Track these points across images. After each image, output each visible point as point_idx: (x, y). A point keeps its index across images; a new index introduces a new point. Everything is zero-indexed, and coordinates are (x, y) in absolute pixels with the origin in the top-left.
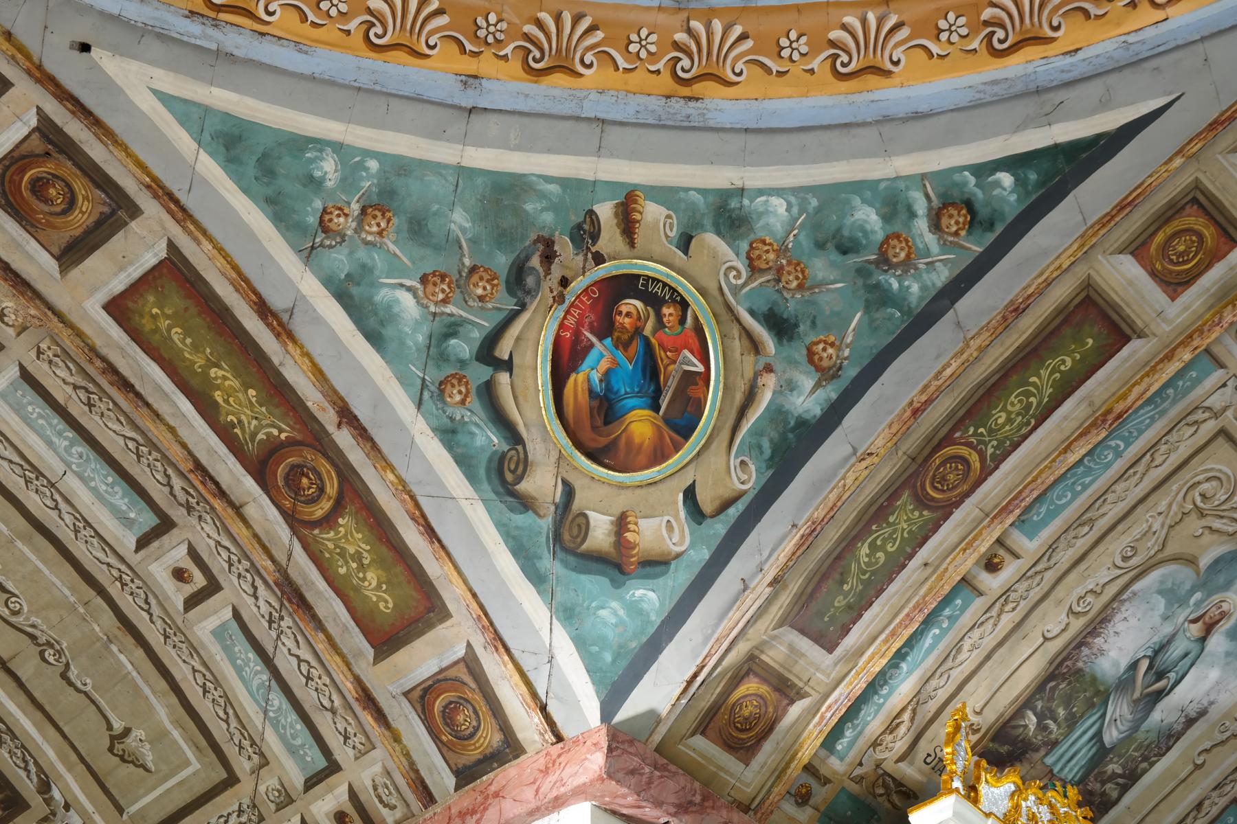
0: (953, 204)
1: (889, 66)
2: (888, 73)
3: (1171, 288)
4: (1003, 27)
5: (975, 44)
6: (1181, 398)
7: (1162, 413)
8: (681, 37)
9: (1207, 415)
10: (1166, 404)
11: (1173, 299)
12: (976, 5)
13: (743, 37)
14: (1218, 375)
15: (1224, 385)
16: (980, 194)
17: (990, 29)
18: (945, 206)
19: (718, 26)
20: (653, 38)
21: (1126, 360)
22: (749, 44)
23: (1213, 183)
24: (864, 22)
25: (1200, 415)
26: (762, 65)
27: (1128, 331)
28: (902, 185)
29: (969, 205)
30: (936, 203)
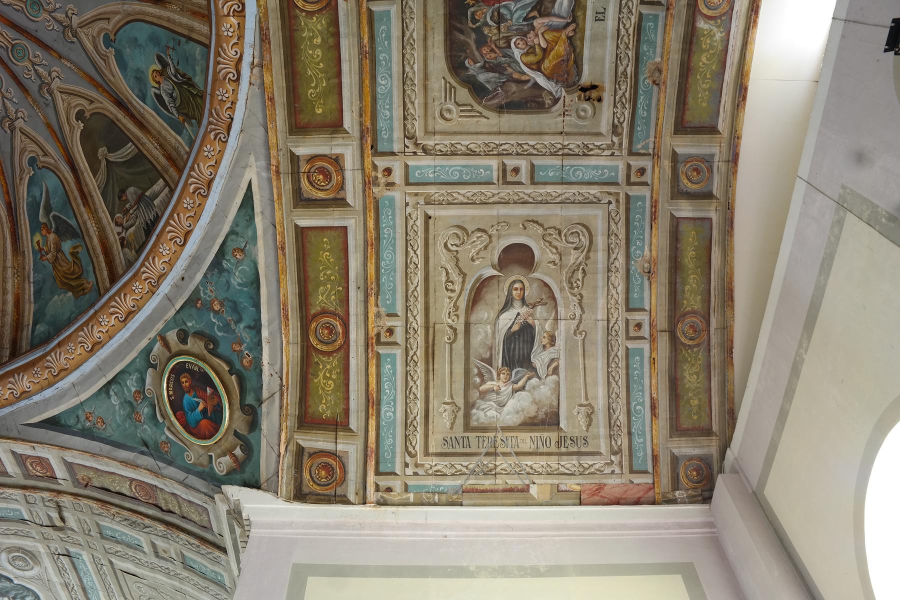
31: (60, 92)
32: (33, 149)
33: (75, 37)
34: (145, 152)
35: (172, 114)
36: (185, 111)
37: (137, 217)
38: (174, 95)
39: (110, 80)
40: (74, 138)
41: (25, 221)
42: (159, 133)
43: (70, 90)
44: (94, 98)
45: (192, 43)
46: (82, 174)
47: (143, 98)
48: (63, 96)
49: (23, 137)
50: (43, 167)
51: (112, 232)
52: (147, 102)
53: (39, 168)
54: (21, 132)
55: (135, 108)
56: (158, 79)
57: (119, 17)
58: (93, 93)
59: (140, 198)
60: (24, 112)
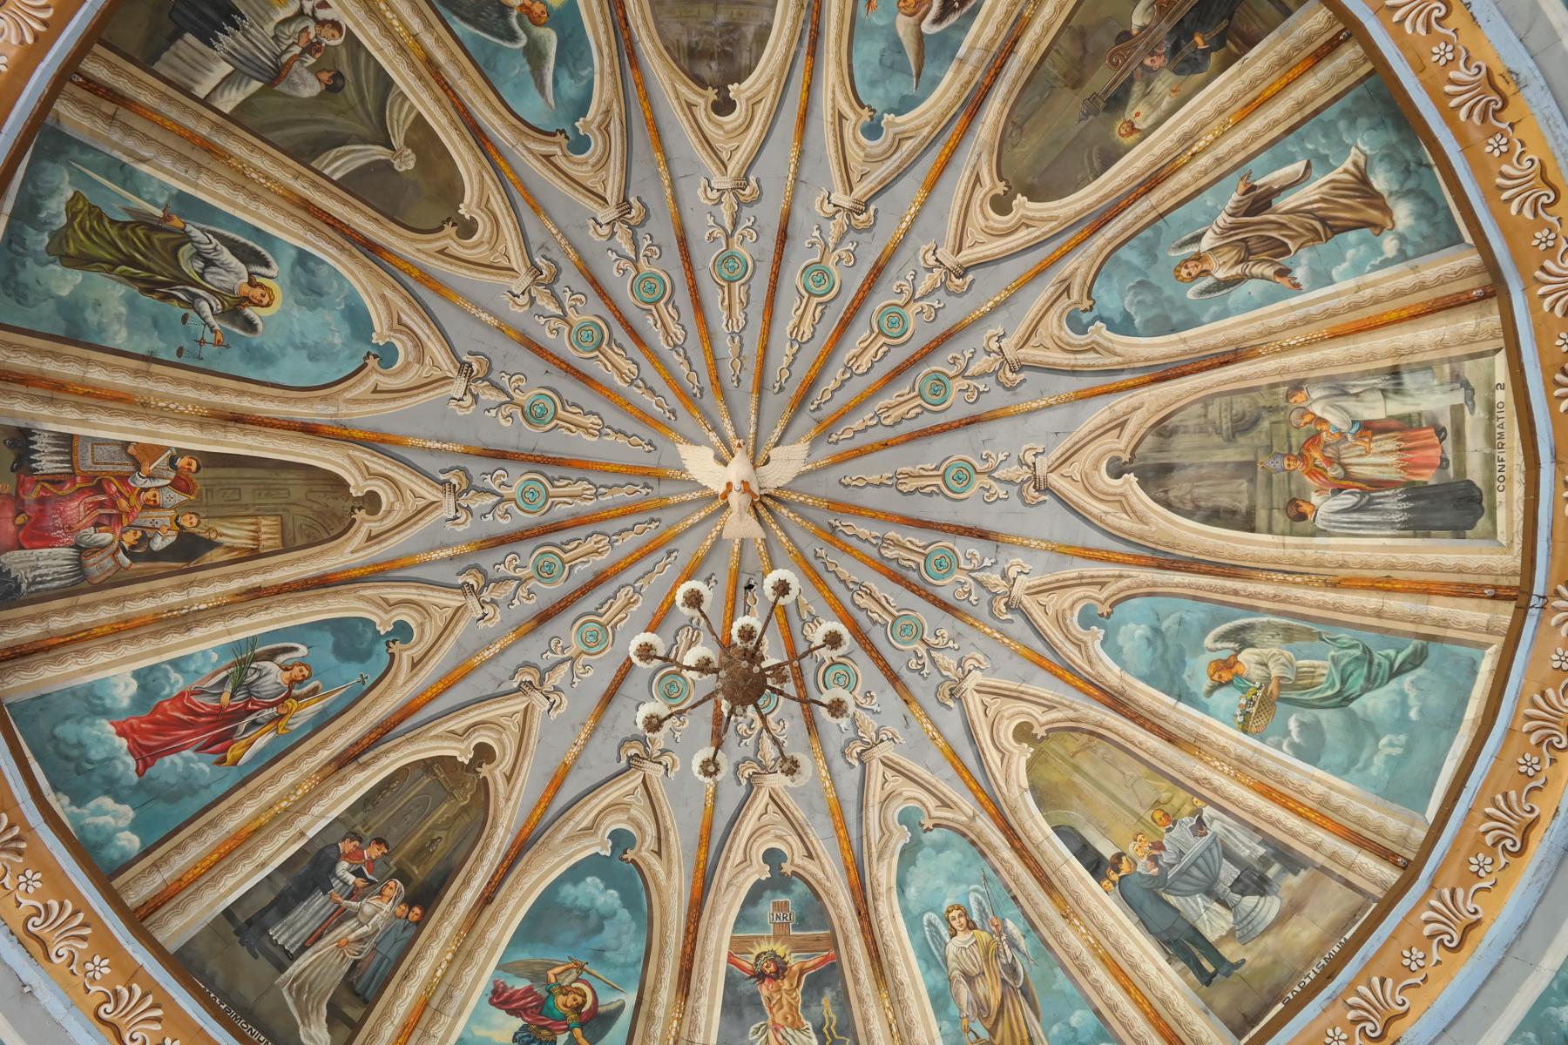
1: (1475, 917)
2: (1478, 922)
4: (1505, 838)
5: (1503, 861)
8: (1351, 1015)
12: (1478, 842)
13: (1383, 981)
17: (1500, 846)
19: (1363, 989)
20: (1338, 1030)
22: (1389, 982)
24: (1433, 909)
26: (1410, 986)
31: (513, 270)
32: (579, 168)
33: (463, 363)
34: (290, 162)
35: (202, 231)
36: (156, 237)
37: (276, 38)
38: (199, 264)
39: (395, 289)
40: (476, 187)
41: (595, 31)
42: (255, 197)
43: (489, 273)
44: (437, 259)
45: (142, 351)
46: (452, 122)
47: (303, 258)
48: (505, 263)
49: (600, 190)
50: (553, 135)
51: (345, 9)
52: (293, 253)
53: (562, 132)
54: (605, 200)
55: (331, 241)
56: (257, 292)
57: (348, 395)
58: (437, 266)
59: (276, 74)
60: (596, 236)
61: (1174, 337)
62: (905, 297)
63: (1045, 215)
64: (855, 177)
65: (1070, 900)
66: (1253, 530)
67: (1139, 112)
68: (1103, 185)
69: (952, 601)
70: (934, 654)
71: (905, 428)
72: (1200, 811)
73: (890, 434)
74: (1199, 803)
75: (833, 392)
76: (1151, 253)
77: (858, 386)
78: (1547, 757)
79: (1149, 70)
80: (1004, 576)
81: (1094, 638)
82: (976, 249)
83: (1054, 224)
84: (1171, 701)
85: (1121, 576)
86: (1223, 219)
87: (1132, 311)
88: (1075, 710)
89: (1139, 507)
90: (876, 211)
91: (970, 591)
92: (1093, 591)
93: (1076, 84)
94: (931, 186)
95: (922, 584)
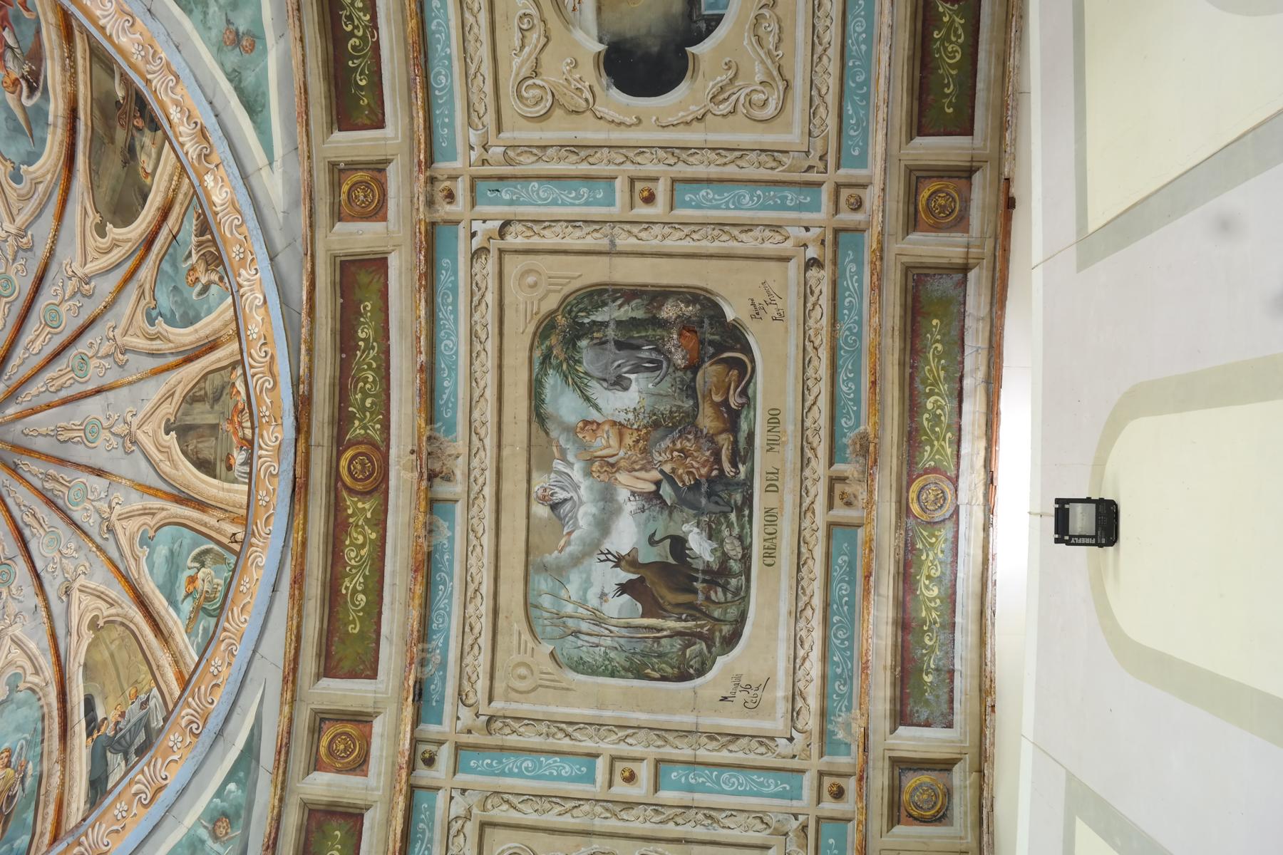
0: (219, 820)
1: (165, 782)
3: (358, 770)
4: (193, 722)
5: (188, 740)
6: (433, 825)
7: (431, 841)
9: (460, 822)
10: (427, 834)
11: (366, 775)
14: (441, 798)
15: (452, 798)
16: (225, 804)
18: (215, 824)
21: (372, 828)
23: (322, 704)
25: (456, 826)
27: (358, 811)
28: (192, 832)
29: (224, 814)
30: (210, 826)
61: (191, 329)
62: (59, 298)
63: (124, 237)
64: (15, 212)
65: (68, 750)
66: (215, 477)
67: (145, 162)
68: (146, 215)
69: (79, 523)
70: (64, 560)
71: (64, 394)
72: (151, 690)
73: (56, 398)
74: (153, 684)
75: (18, 366)
76: (174, 265)
77: (37, 361)
78: (227, 660)
79: (139, 129)
80: (110, 507)
81: (143, 553)
82: (94, 264)
83: (130, 244)
84: (166, 603)
85: (163, 509)
86: (194, 239)
87: (174, 308)
88: (122, 608)
89: (175, 457)
90: (32, 235)
91: (90, 517)
92: (148, 519)
93: (112, 140)
94: (60, 217)
95: (65, 508)
